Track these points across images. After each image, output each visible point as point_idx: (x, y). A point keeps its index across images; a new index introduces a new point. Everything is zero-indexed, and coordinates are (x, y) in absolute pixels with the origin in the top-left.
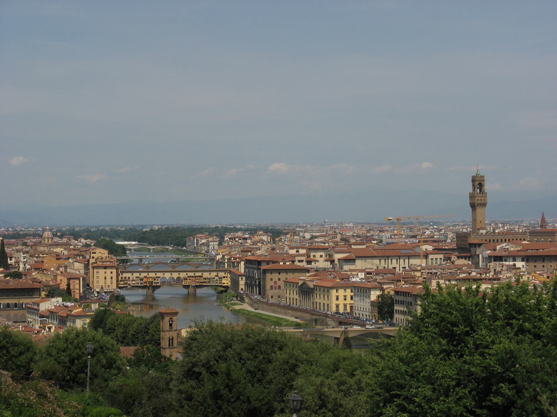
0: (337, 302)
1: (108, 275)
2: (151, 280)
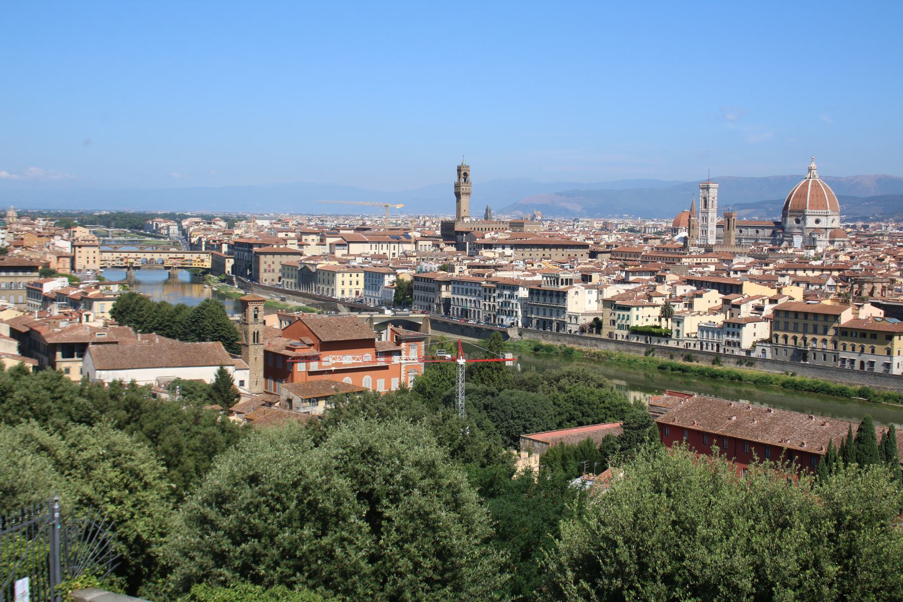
0: (343, 287)
1: (91, 256)
2: (131, 260)
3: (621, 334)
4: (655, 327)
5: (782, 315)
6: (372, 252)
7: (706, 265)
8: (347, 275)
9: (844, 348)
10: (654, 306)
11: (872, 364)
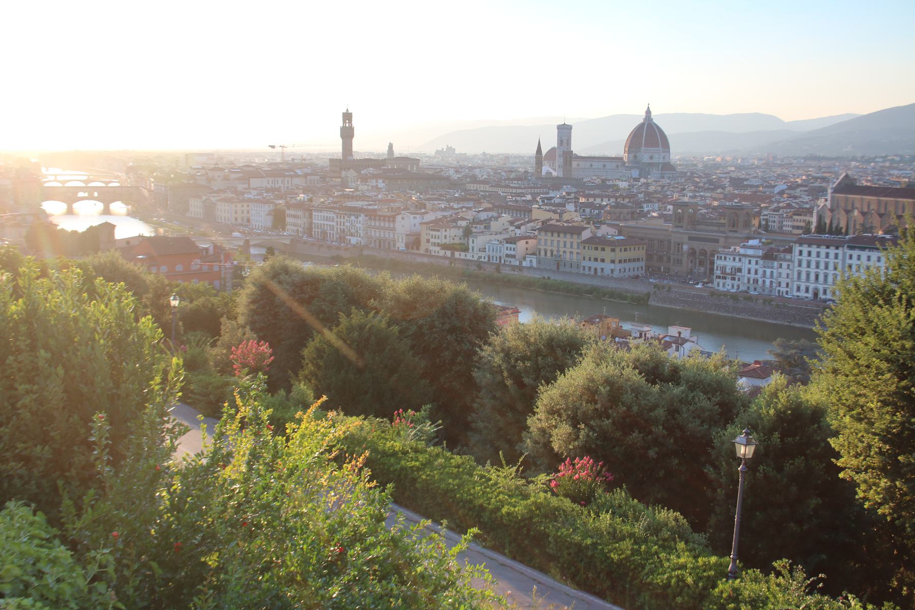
3: (435, 250)
4: (460, 244)
5: (543, 233)
6: (269, 186)
7: (523, 195)
8: (239, 205)
10: (459, 227)
11: (602, 269)
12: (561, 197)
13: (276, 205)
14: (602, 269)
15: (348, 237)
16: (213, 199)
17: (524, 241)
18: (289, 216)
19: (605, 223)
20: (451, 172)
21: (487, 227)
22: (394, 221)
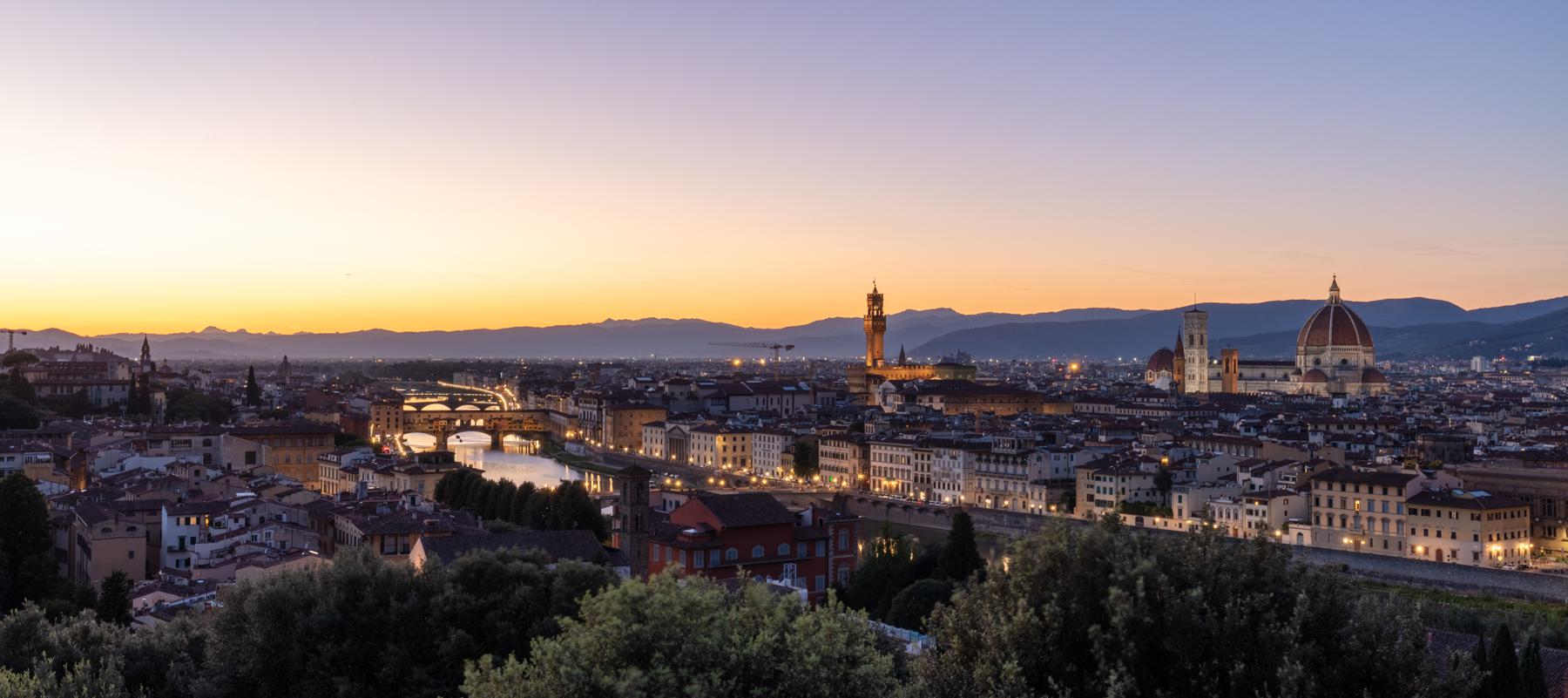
5: (1324, 485)
6: (759, 408)
9: (1413, 531)
10: (1145, 475)
12: (1275, 423)
13: (797, 436)
14: (1454, 553)
15: (936, 491)
16: (686, 429)
17: (1281, 499)
18: (825, 454)
19: (1440, 468)
20: (1032, 385)
21: (1192, 472)
22: (1024, 463)
